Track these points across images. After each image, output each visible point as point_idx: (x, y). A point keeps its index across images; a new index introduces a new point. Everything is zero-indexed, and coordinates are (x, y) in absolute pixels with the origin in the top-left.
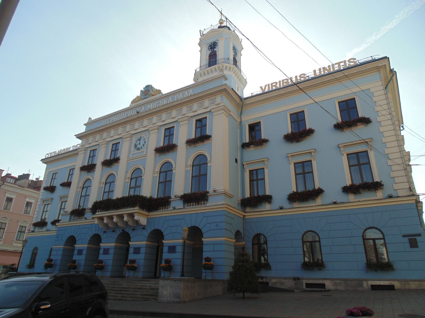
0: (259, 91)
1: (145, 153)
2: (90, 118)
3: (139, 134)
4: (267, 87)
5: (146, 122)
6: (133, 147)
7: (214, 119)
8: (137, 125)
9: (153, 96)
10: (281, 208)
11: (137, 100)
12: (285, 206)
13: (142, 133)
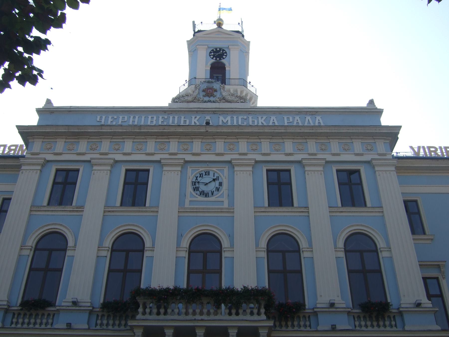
0: (410, 154)
1: (226, 205)
2: (49, 102)
4: (422, 150)
5: (220, 146)
6: (190, 189)
7: (378, 177)
8: (197, 145)
11: (190, 99)
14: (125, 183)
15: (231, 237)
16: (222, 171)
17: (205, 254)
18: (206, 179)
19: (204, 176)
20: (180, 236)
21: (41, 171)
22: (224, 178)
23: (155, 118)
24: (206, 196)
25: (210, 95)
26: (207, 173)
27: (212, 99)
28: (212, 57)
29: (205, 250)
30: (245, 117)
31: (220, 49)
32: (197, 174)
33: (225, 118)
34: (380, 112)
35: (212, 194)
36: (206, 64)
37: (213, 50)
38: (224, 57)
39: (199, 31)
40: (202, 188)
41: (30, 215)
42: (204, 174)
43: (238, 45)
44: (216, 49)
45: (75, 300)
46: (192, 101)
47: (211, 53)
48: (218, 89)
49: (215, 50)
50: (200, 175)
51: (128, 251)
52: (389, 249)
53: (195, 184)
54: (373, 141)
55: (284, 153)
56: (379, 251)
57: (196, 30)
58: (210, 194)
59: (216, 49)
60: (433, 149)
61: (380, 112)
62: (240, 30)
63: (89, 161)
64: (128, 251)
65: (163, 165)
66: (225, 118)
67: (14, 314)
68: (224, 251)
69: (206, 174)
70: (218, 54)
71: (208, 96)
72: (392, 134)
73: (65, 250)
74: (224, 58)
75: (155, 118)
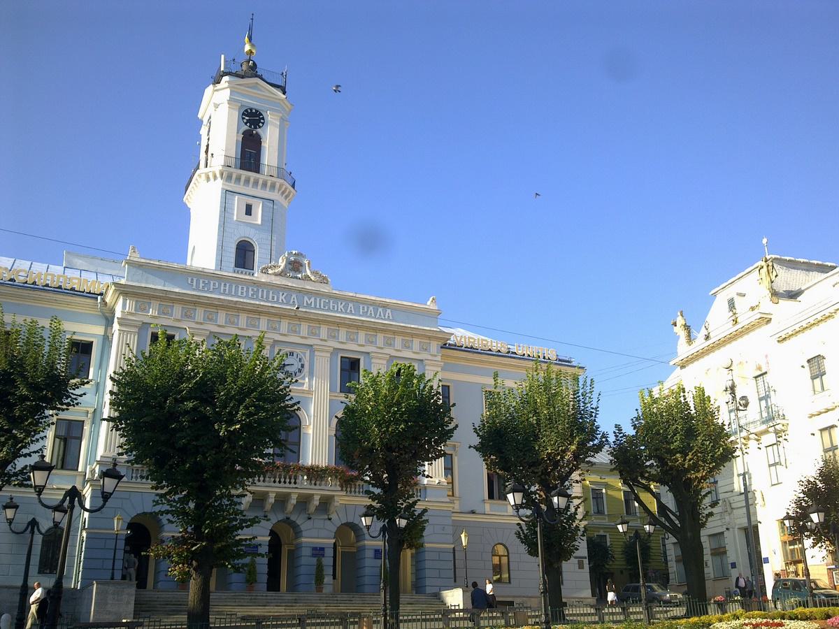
10: (473, 512)
12: (477, 512)
16: (304, 354)
23: (245, 289)
30: (327, 301)
31: (257, 111)
47: (243, 114)
49: (249, 111)
58: (293, 374)
59: (251, 110)
60: (473, 340)
70: (253, 118)
74: (260, 127)
75: (245, 289)
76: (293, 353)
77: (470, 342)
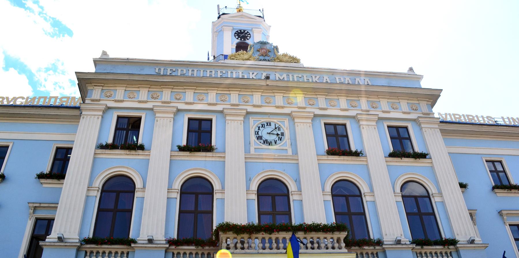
1: (290, 152)
3: (267, 117)
6: (253, 138)
8: (257, 98)
9: (281, 61)
13: (271, 117)
14: (189, 131)
15: (298, 181)
17: (273, 197)
18: (269, 129)
19: (266, 127)
20: (249, 180)
21: (102, 117)
22: (285, 129)
23: (213, 72)
24: (269, 144)
25: (264, 54)
26: (269, 124)
27: (267, 58)
28: (237, 37)
29: (273, 194)
31: (244, 31)
32: (259, 124)
33: (281, 76)
34: (420, 77)
35: (276, 143)
36: (232, 43)
37: (237, 32)
38: (248, 38)
39: (224, 14)
40: (266, 137)
41: (94, 158)
42: (266, 124)
43: (260, 28)
44: (240, 31)
45: (151, 238)
46: (248, 59)
47: (235, 33)
48: (272, 50)
50: (262, 125)
51: (196, 195)
52: (440, 194)
53: (258, 134)
54: (417, 102)
55: (338, 110)
56: (431, 197)
57: (221, 13)
58: (273, 143)
59: (240, 31)
60: (458, 116)
61: (420, 77)
62: (262, 16)
63: (152, 109)
64: (196, 195)
65: (226, 114)
66: (281, 76)
67: (86, 252)
68: (292, 194)
69: (267, 125)
71: (263, 55)
72: (433, 96)
73: (133, 192)
74: (248, 39)
75: (213, 72)
76: (270, 124)
77: (455, 118)
